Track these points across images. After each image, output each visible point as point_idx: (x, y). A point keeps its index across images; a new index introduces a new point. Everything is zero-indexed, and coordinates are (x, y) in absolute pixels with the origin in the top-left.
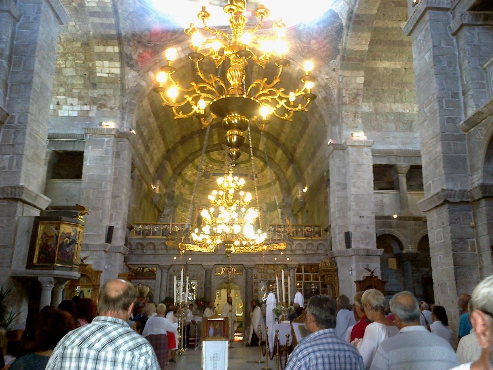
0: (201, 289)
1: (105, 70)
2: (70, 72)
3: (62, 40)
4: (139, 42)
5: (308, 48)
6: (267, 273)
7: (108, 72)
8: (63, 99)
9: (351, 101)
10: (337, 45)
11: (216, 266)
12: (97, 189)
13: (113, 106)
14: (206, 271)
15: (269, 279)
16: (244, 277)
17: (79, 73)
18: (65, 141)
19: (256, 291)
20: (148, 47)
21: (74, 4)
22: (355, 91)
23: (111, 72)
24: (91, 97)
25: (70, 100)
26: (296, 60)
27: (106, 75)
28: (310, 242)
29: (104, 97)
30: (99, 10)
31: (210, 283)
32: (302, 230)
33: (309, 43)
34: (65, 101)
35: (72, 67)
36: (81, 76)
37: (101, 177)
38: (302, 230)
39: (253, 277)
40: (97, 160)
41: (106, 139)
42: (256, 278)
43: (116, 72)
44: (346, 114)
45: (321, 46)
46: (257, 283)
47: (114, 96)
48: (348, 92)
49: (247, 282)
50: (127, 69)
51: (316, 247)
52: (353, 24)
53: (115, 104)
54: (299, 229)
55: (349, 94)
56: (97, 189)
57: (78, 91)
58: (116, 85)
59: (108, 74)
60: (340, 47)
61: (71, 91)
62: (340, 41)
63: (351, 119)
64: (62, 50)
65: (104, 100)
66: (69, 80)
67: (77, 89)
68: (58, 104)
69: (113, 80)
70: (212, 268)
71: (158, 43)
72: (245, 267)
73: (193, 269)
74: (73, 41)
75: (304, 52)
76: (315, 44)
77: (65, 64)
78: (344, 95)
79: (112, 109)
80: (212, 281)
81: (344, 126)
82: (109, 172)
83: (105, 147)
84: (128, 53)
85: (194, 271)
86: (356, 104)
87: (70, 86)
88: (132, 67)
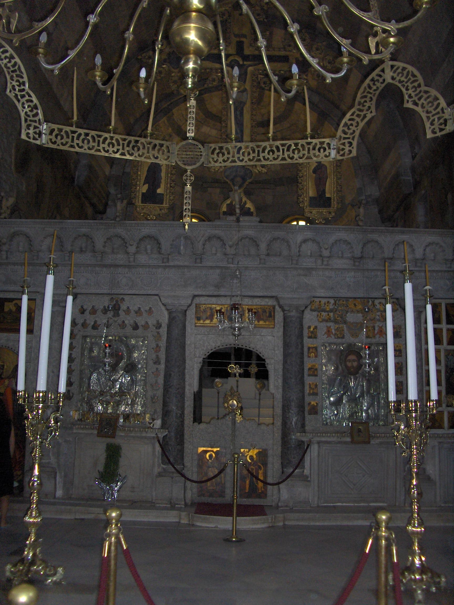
0: (157, 362)
6: (345, 322)
11: (197, 300)
14: (170, 313)
15: (349, 339)
16: (279, 331)
19: (314, 372)
31: (183, 347)
39: (306, 333)
42: (313, 335)
46: (316, 348)
49: (286, 345)
72: (281, 302)
73: (136, 308)
80: (188, 342)
85: (136, 312)
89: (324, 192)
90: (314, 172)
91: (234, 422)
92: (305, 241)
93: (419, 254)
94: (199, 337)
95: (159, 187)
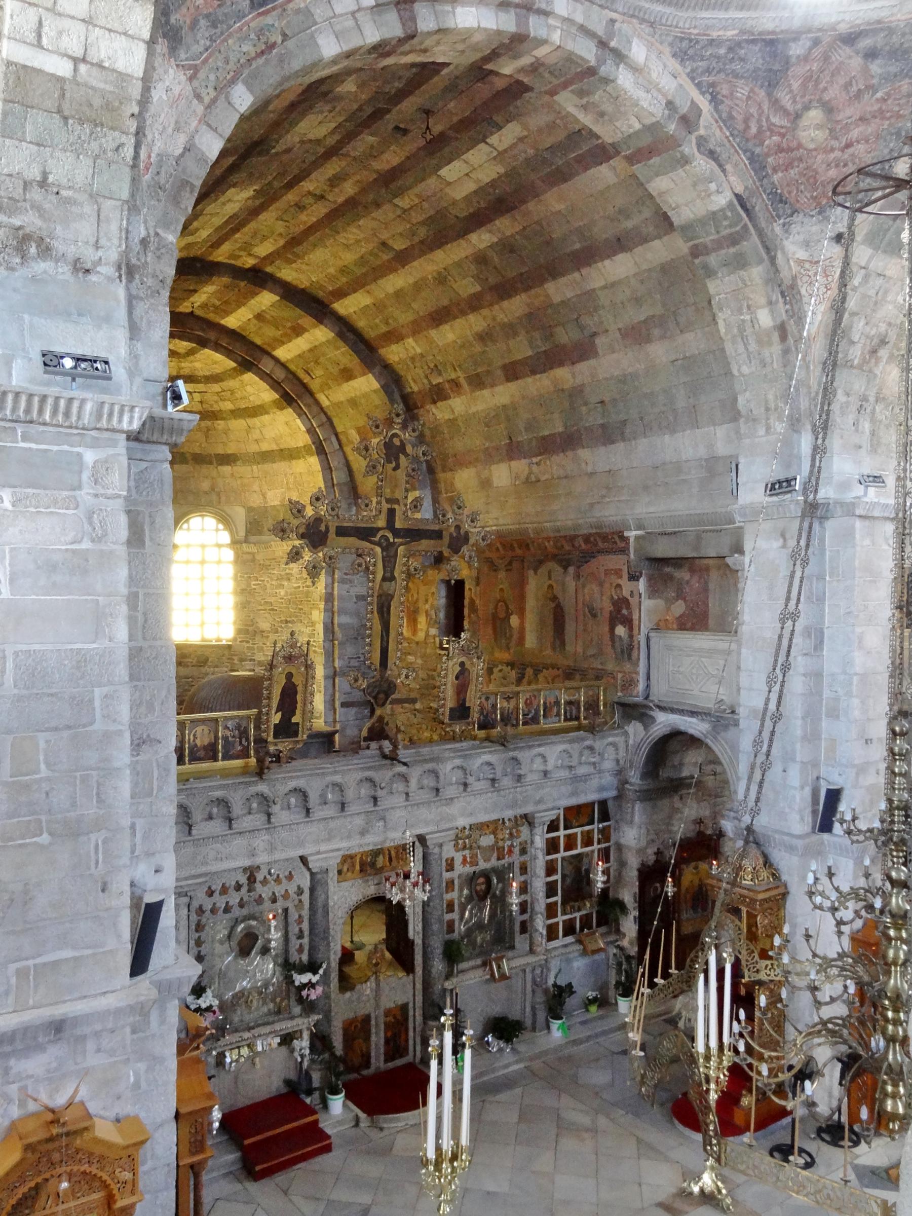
1: (60, 33)
5: (783, 136)
7: (79, 53)
12: (69, 727)
13: (89, 255)
22: (883, 327)
23: (93, 56)
26: (728, 167)
27: (64, 68)
29: (36, 194)
37: (82, 660)
40: (53, 568)
41: (90, 456)
43: (120, 66)
47: (94, 197)
53: (97, 246)
56: (69, 727)
58: (110, 139)
59: (76, 61)
69: (97, 102)
75: (762, 144)
79: (81, 269)
82: (121, 631)
83: (85, 495)
86: (870, 371)
89: (464, 700)
95: (294, 714)
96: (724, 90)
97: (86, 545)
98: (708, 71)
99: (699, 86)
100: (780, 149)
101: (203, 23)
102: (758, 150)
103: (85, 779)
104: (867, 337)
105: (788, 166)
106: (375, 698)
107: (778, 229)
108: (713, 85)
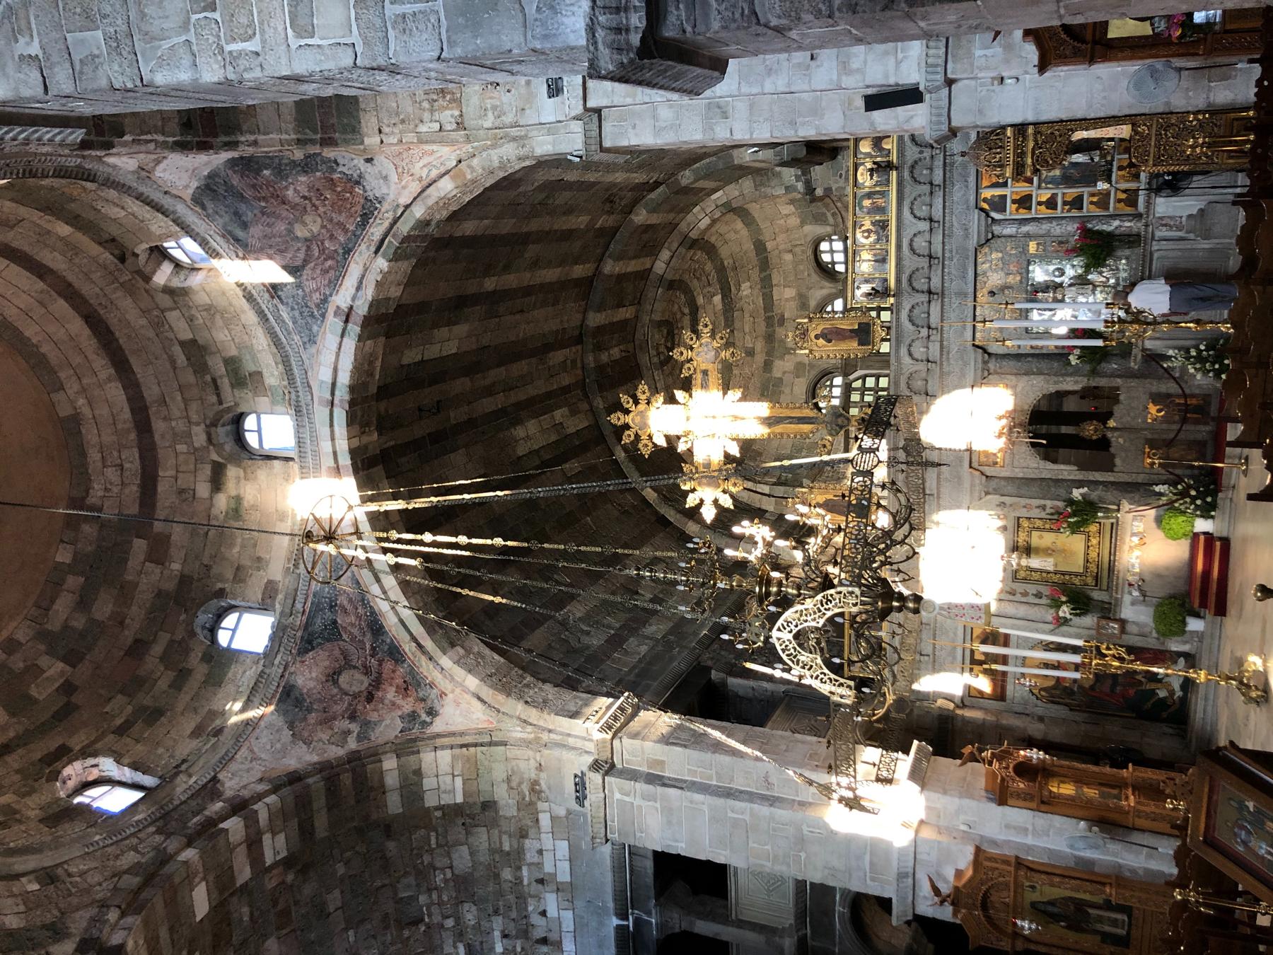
2: (461, 857)
3: (387, 882)
4: (370, 698)
8: (529, 870)
9: (453, 100)
10: (294, 164)
11: (975, 465)
13: (532, 763)
17: (462, 837)
18: (631, 875)
20: (380, 674)
21: (290, 878)
24: (519, 809)
25: (530, 857)
28: (906, 174)
30: (294, 823)
32: (869, 195)
33: (306, 240)
34: (533, 868)
35: (449, 855)
36: (468, 833)
37: (713, 819)
38: (869, 195)
41: (617, 796)
44: (490, 114)
45: (309, 206)
48: (426, 116)
50: (438, 726)
51: (921, 152)
52: (216, 136)
54: (867, 203)
55: (432, 111)
57: (505, 838)
60: (299, 154)
61: (508, 854)
62: (281, 158)
63: (506, 98)
64: (411, 880)
65: (520, 784)
66: (482, 859)
67: (501, 843)
68: (541, 881)
70: (982, 474)
71: (368, 646)
74: (384, 857)
75: (335, 251)
76: (305, 224)
77: (442, 869)
78: (436, 126)
80: (1021, 475)
81: (530, 118)
84: (399, 725)
87: (497, 858)
88: (432, 712)
89: (851, 331)
90: (829, 341)
91: (1115, 429)
92: (910, 354)
93: (924, 226)
94: (1016, 463)
96: (316, 297)
97: (658, 805)
98: (312, 316)
99: (323, 315)
100: (332, 237)
101: (421, 695)
102: (341, 251)
103: (774, 830)
104: (432, 111)
105: (340, 224)
106: (841, 427)
107: (386, 206)
108: (318, 306)
